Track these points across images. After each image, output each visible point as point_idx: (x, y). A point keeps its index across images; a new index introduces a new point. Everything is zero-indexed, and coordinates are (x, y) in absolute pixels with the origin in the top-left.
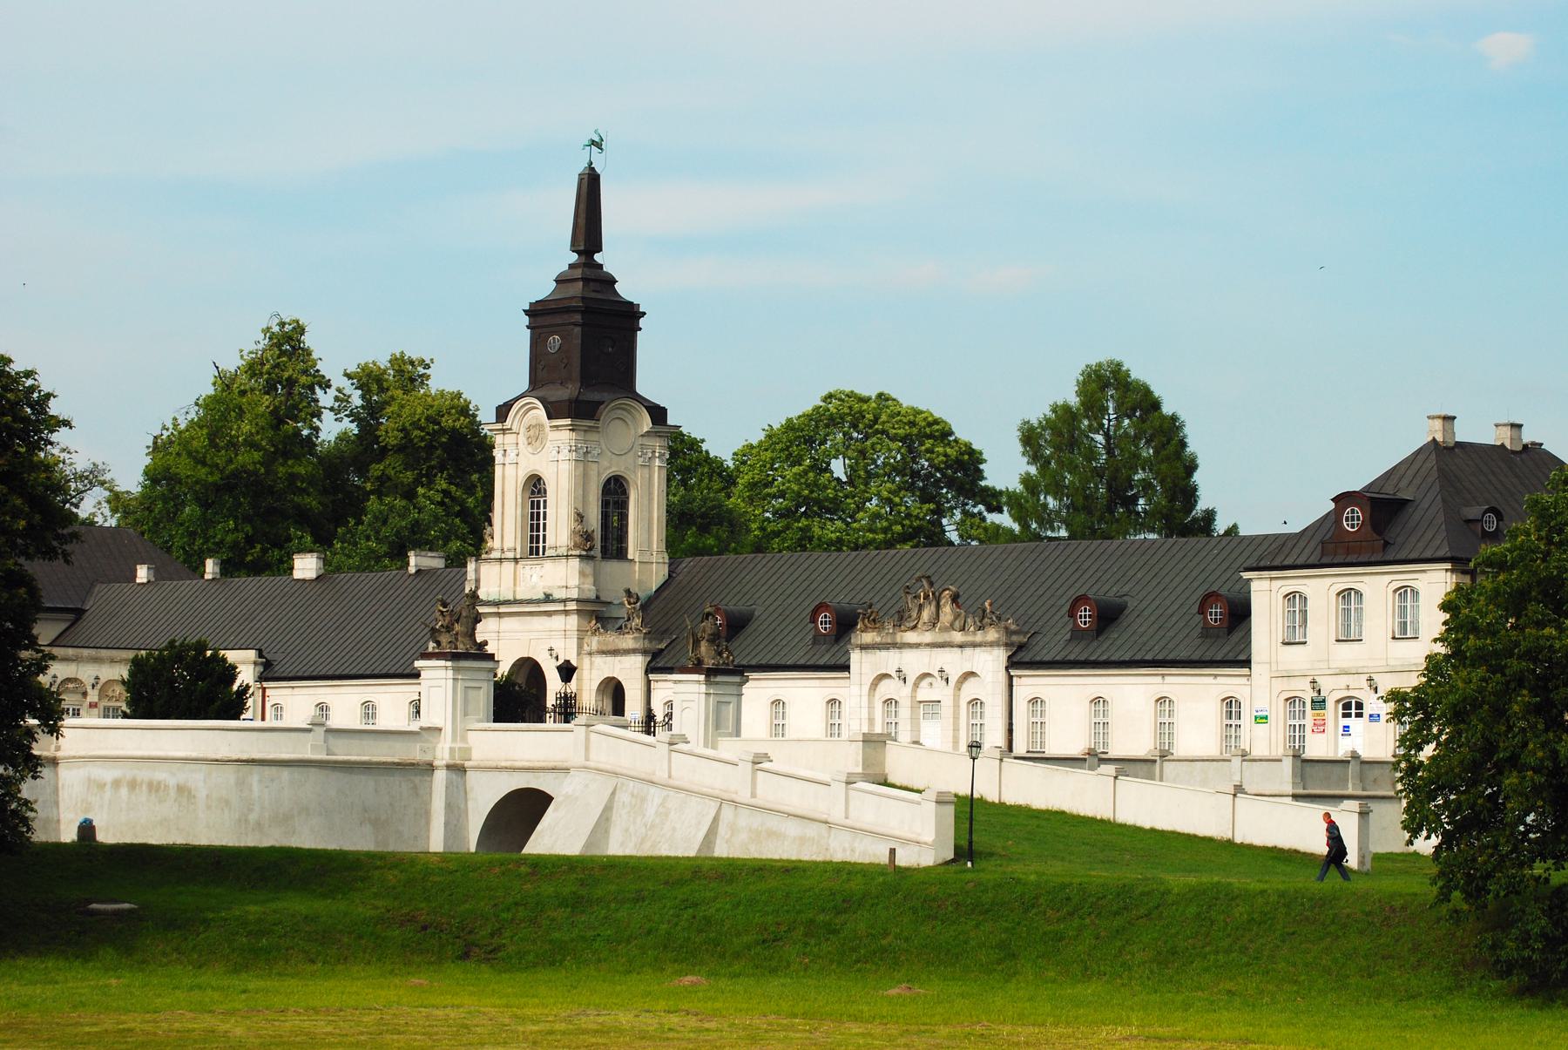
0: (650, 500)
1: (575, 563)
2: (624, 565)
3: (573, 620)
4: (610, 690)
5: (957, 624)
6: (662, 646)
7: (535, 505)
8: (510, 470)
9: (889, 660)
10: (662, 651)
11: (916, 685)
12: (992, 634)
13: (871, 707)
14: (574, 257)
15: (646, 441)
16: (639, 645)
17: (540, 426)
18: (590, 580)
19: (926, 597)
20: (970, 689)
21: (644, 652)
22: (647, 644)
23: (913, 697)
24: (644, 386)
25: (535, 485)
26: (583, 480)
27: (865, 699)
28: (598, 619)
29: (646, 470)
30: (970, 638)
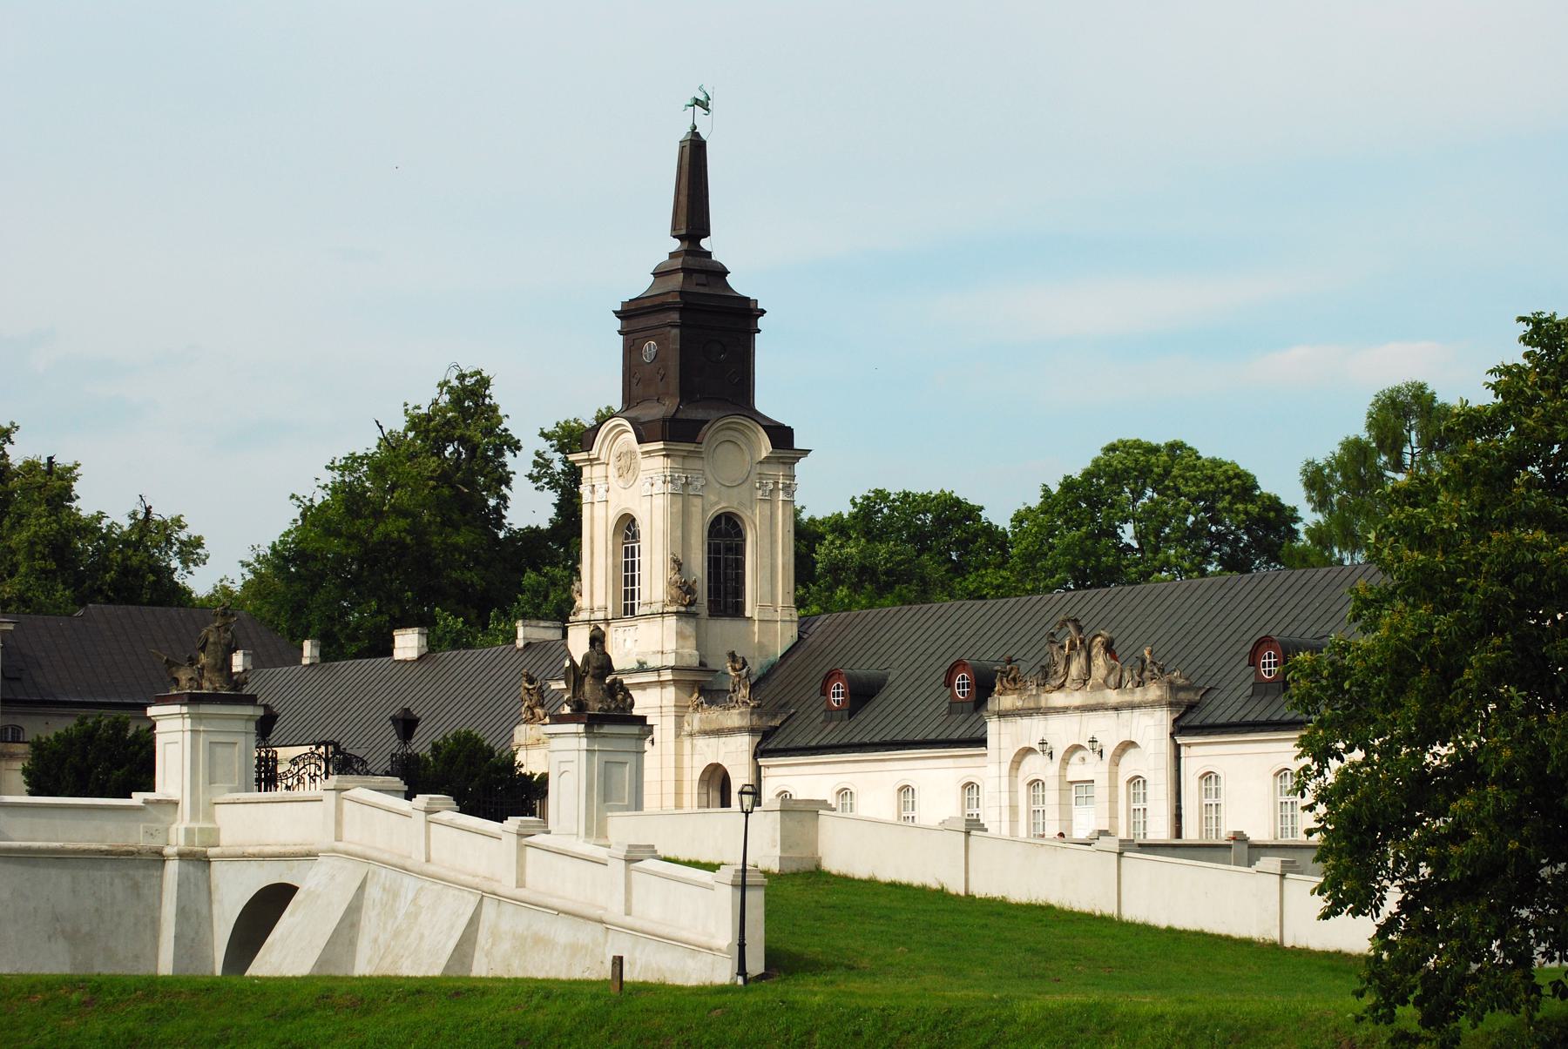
0: (773, 542)
1: (672, 621)
3: (670, 693)
4: (717, 782)
5: (1112, 680)
6: (777, 722)
7: (631, 552)
8: (599, 509)
9: (1031, 730)
10: (777, 728)
11: (1065, 761)
12: (1154, 692)
13: (1012, 791)
14: (676, 244)
15: (767, 470)
16: (745, 722)
17: (632, 453)
18: (692, 642)
19: (1073, 646)
20: (1131, 764)
21: (752, 731)
22: (756, 721)
23: (1062, 776)
24: (764, 403)
25: (627, 527)
26: (682, 519)
27: (1005, 781)
28: (702, 692)
29: (767, 506)
30: (1127, 698)
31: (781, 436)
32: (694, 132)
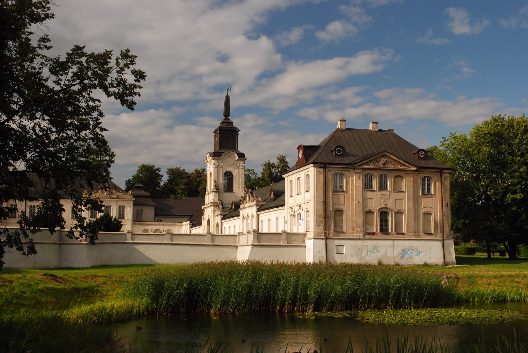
2: (231, 194)
6: (227, 213)
10: (226, 215)
14: (224, 118)
15: (237, 162)
21: (221, 215)
29: (238, 170)
32: (227, 95)
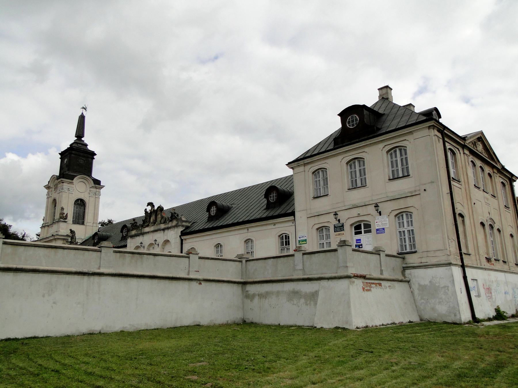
15: (91, 189)
30: (167, 226)
31: (97, 182)
32: (82, 113)
